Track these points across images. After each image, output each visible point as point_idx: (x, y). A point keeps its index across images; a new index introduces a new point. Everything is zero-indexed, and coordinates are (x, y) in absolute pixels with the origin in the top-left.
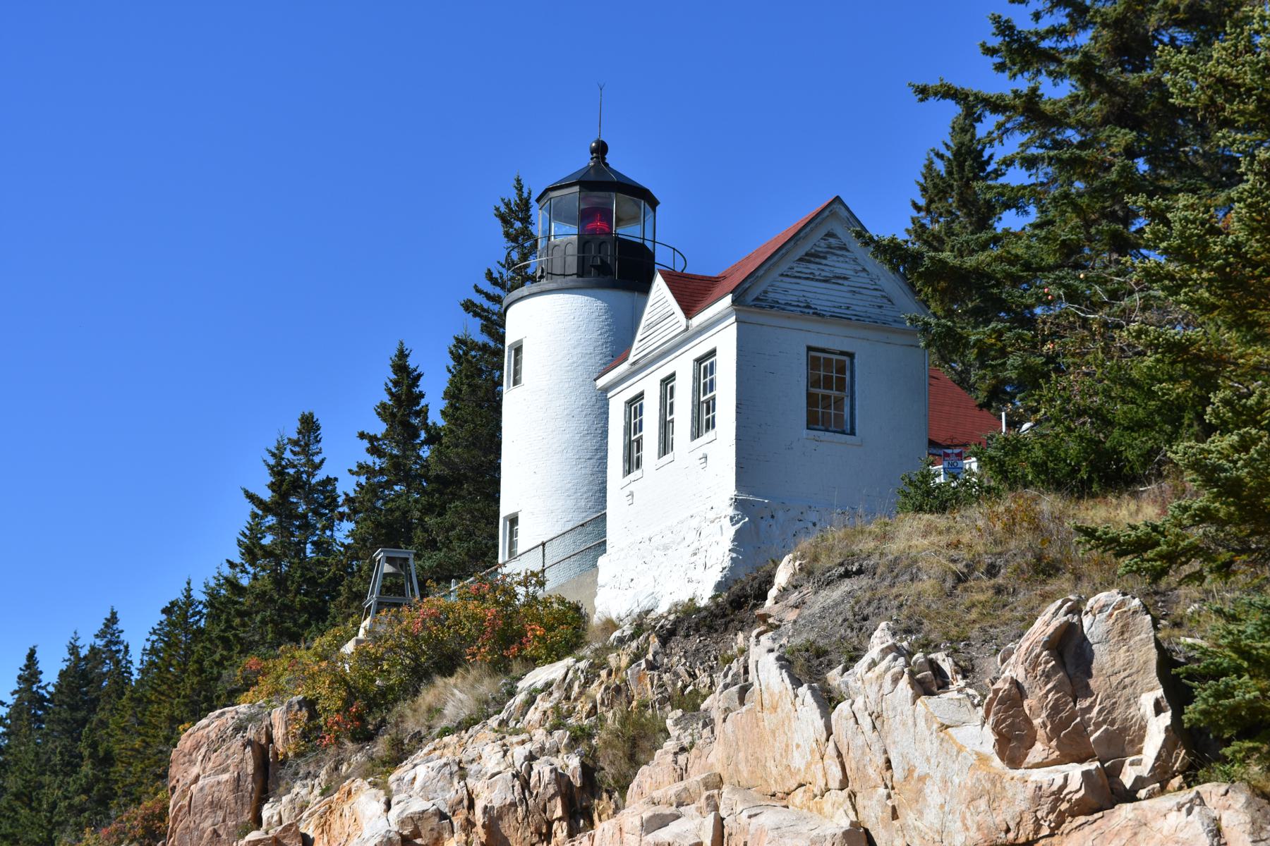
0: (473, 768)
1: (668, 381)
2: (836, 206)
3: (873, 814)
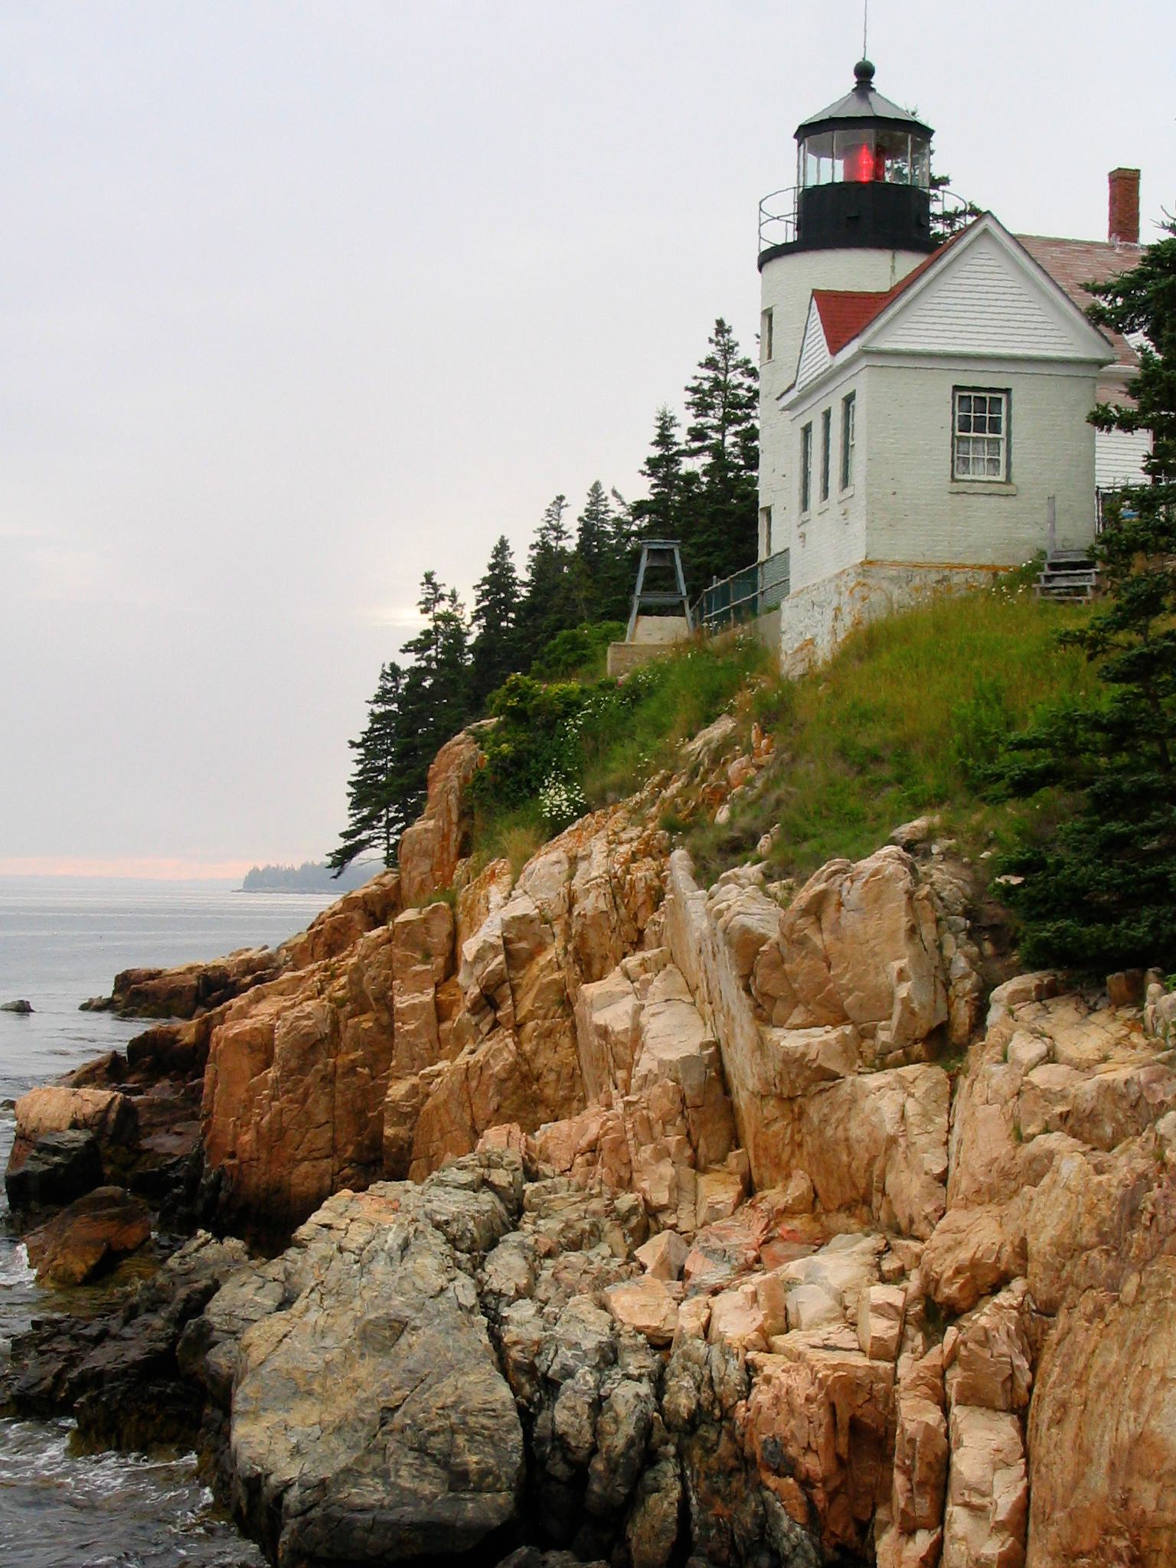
1: (827, 415)
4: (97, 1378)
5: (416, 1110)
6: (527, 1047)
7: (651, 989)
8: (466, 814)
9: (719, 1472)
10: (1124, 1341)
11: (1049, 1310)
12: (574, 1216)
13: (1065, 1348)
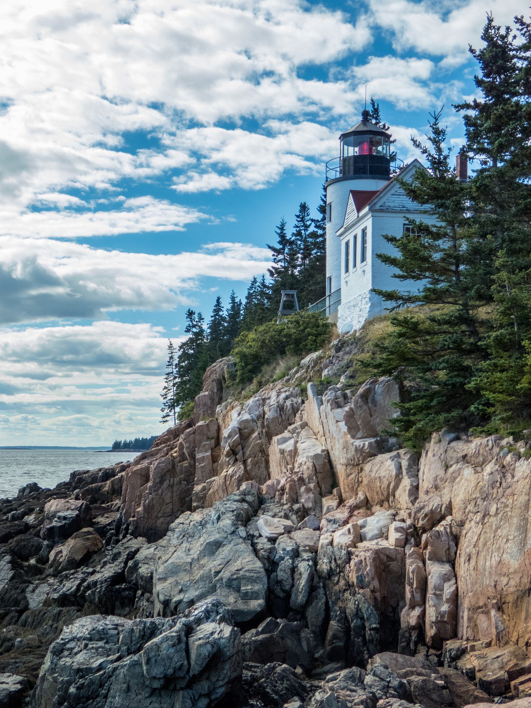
0: (268, 401)
1: (355, 237)
2: (415, 163)
3: (329, 448)
4: (95, 583)
5: (205, 496)
6: (248, 468)
7: (301, 435)
8: (220, 389)
9: (340, 591)
10: (492, 528)
11: (462, 524)
12: (278, 511)
13: (469, 535)
